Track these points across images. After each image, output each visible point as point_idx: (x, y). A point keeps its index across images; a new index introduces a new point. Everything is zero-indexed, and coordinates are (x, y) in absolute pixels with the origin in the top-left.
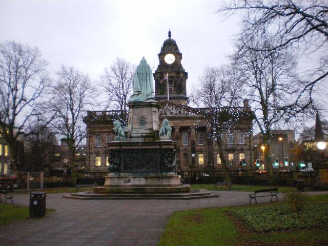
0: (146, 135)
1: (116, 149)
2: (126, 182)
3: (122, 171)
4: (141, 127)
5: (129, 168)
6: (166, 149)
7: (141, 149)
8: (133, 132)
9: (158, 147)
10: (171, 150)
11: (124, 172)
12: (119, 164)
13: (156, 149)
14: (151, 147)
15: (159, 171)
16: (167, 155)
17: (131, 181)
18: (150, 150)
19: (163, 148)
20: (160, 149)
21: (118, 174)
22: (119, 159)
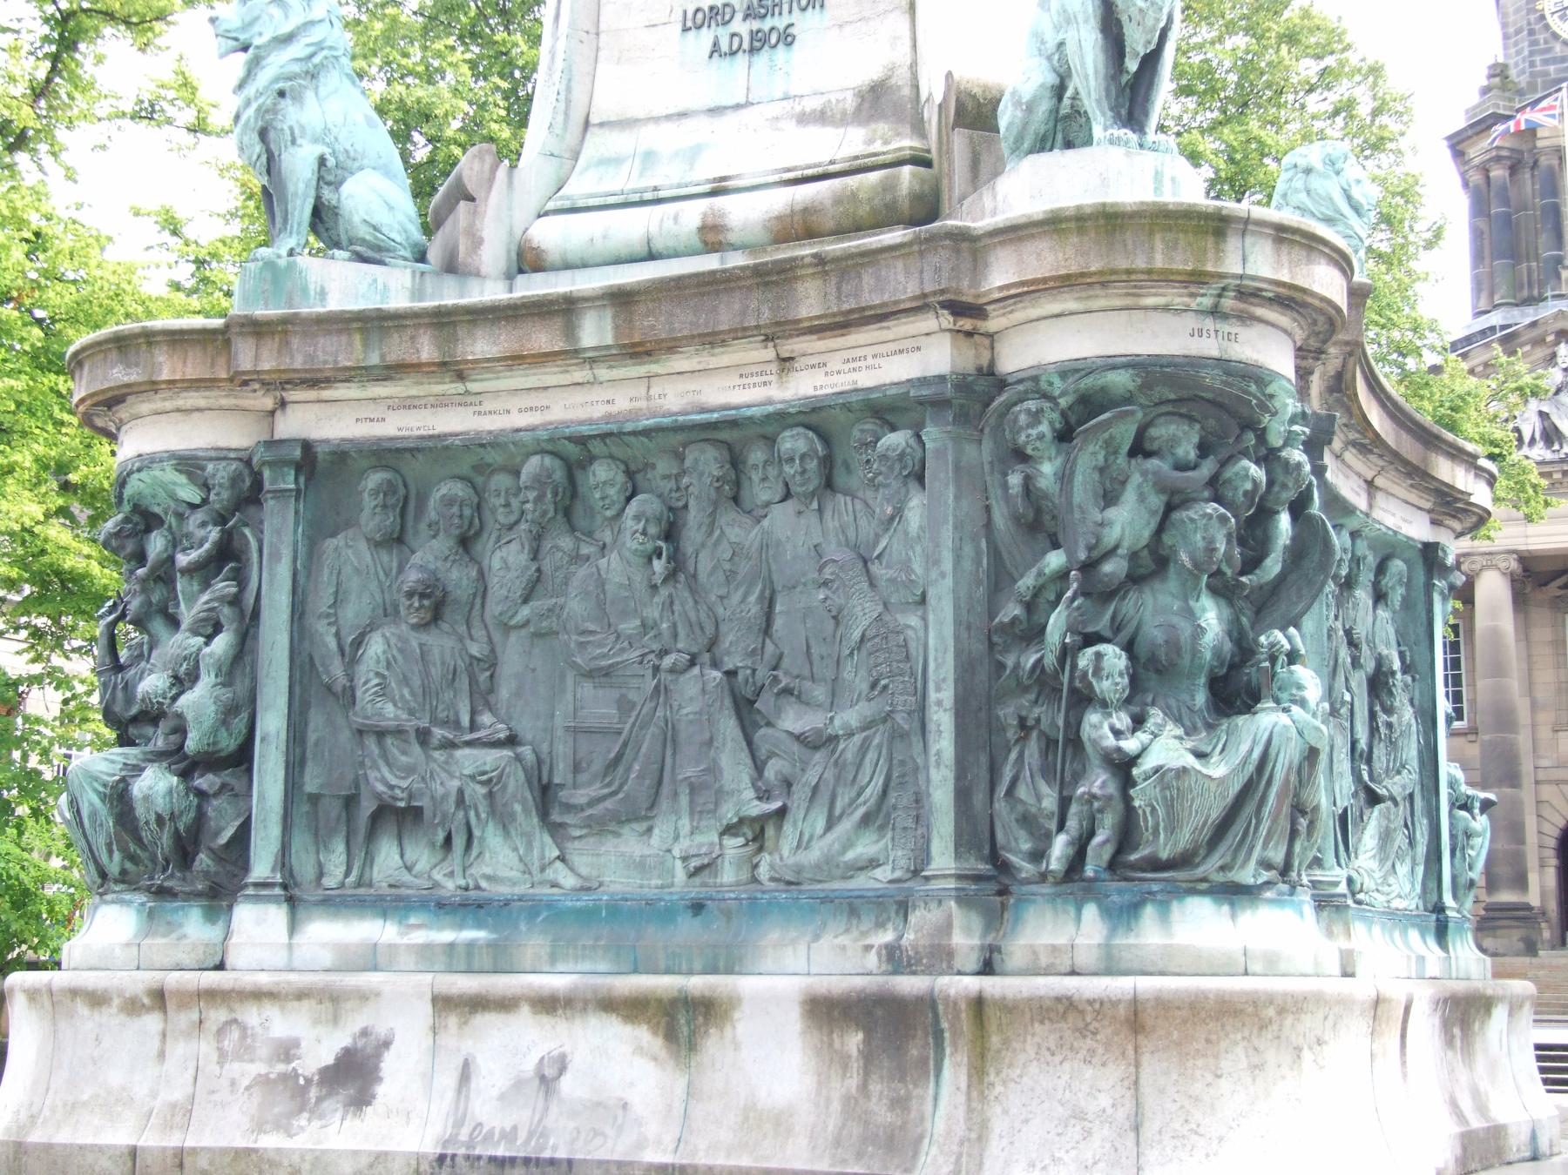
0: (781, 200)
1: (188, 464)
2: (295, 1093)
3: (262, 866)
4: (732, 78)
5: (401, 817)
6: (1084, 406)
7: (634, 449)
8: (580, 187)
9: (919, 355)
10: (1222, 409)
11: (293, 896)
12: (242, 758)
13: (884, 409)
14: (806, 385)
15: (943, 858)
16: (1127, 522)
17: (398, 1074)
18: (793, 442)
19: (1033, 383)
20: (977, 397)
21: (195, 927)
22: (222, 643)
